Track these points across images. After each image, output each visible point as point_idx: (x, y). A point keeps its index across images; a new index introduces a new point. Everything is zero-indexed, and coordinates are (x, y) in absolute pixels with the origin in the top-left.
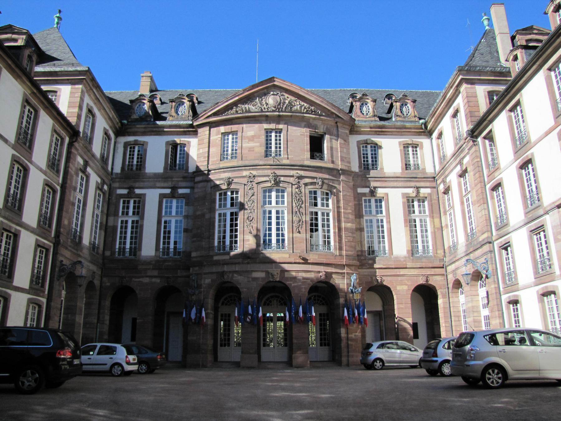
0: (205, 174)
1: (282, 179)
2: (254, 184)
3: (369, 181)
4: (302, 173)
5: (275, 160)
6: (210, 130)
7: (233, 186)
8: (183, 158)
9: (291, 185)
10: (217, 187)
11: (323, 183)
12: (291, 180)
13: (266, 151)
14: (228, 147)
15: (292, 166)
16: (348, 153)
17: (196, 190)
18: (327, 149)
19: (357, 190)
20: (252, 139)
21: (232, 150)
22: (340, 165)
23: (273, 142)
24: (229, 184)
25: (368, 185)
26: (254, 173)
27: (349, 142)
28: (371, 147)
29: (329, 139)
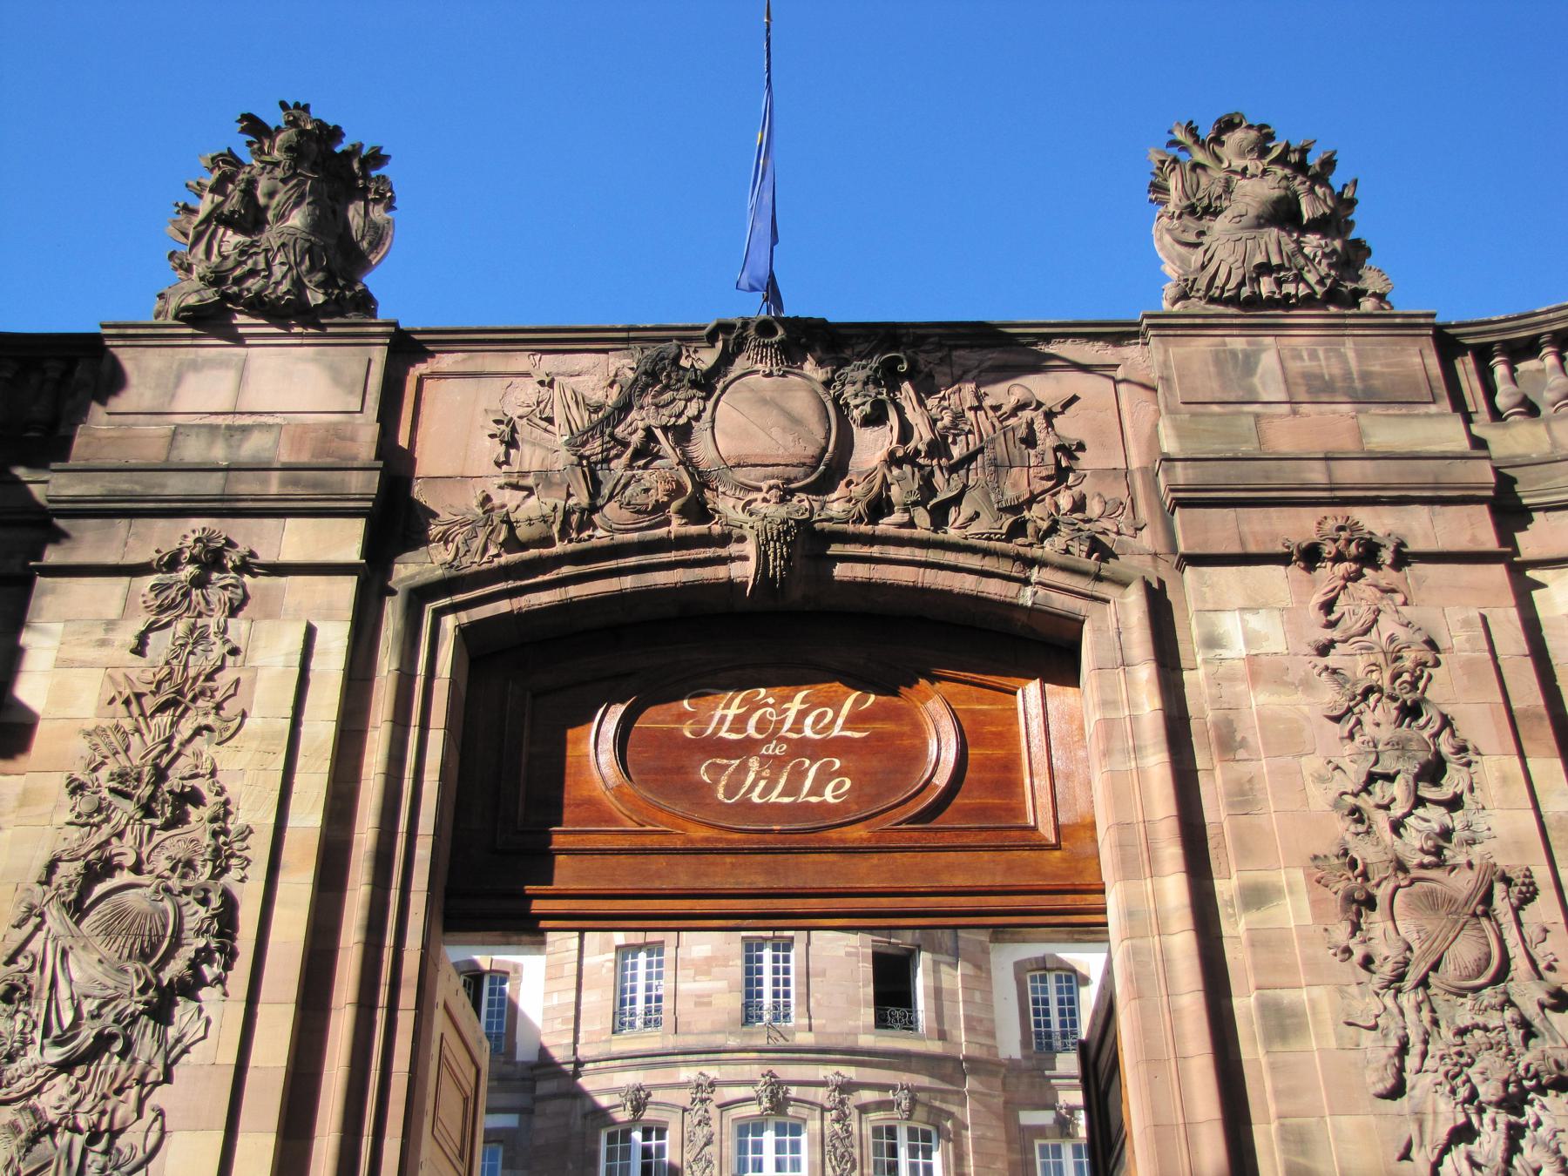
0: (564, 1073)
1: (794, 1091)
2: (711, 1107)
3: (1052, 1087)
4: (850, 1073)
5: (774, 1034)
6: (581, 939)
7: (649, 1114)
8: (500, 1014)
9: (818, 1113)
10: (600, 1116)
11: (914, 1102)
12: (820, 1095)
13: (747, 1006)
14: (633, 990)
15: (821, 1054)
16: (988, 1005)
17: (538, 1123)
18: (926, 996)
19: (1017, 1118)
20: (704, 967)
21: (648, 1000)
22: (963, 1044)
23: (767, 976)
24: (639, 1106)
25: (1049, 1100)
26: (713, 1072)
27: (989, 971)
28: (1059, 979)
29: (930, 963)
